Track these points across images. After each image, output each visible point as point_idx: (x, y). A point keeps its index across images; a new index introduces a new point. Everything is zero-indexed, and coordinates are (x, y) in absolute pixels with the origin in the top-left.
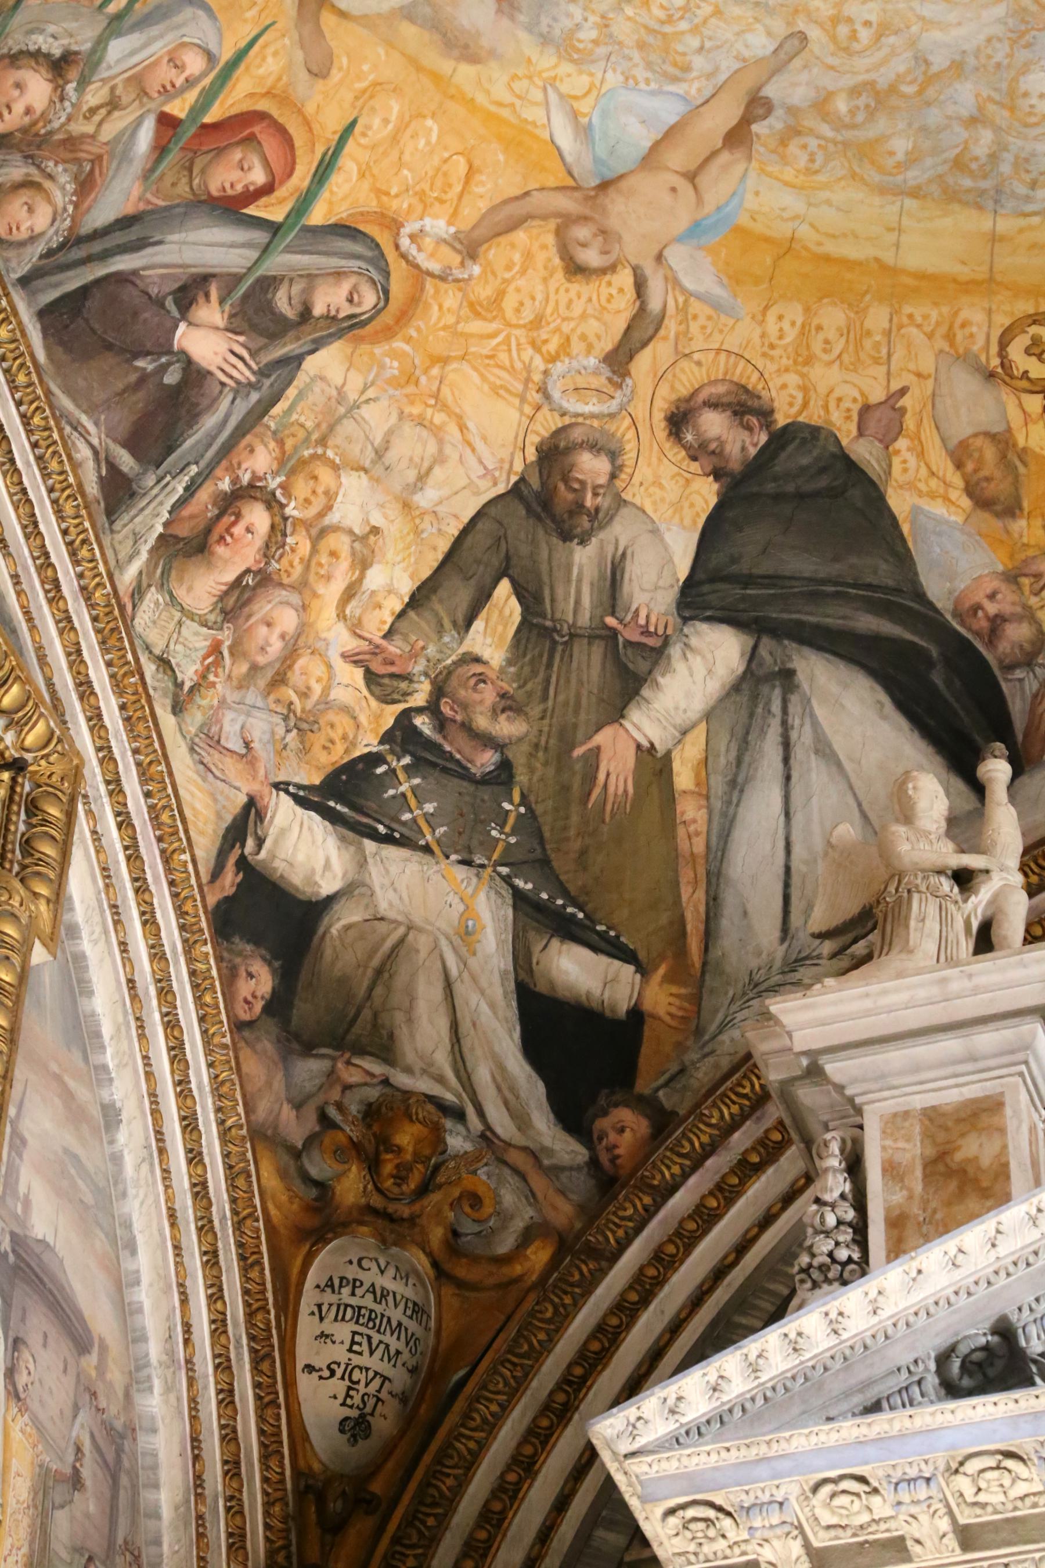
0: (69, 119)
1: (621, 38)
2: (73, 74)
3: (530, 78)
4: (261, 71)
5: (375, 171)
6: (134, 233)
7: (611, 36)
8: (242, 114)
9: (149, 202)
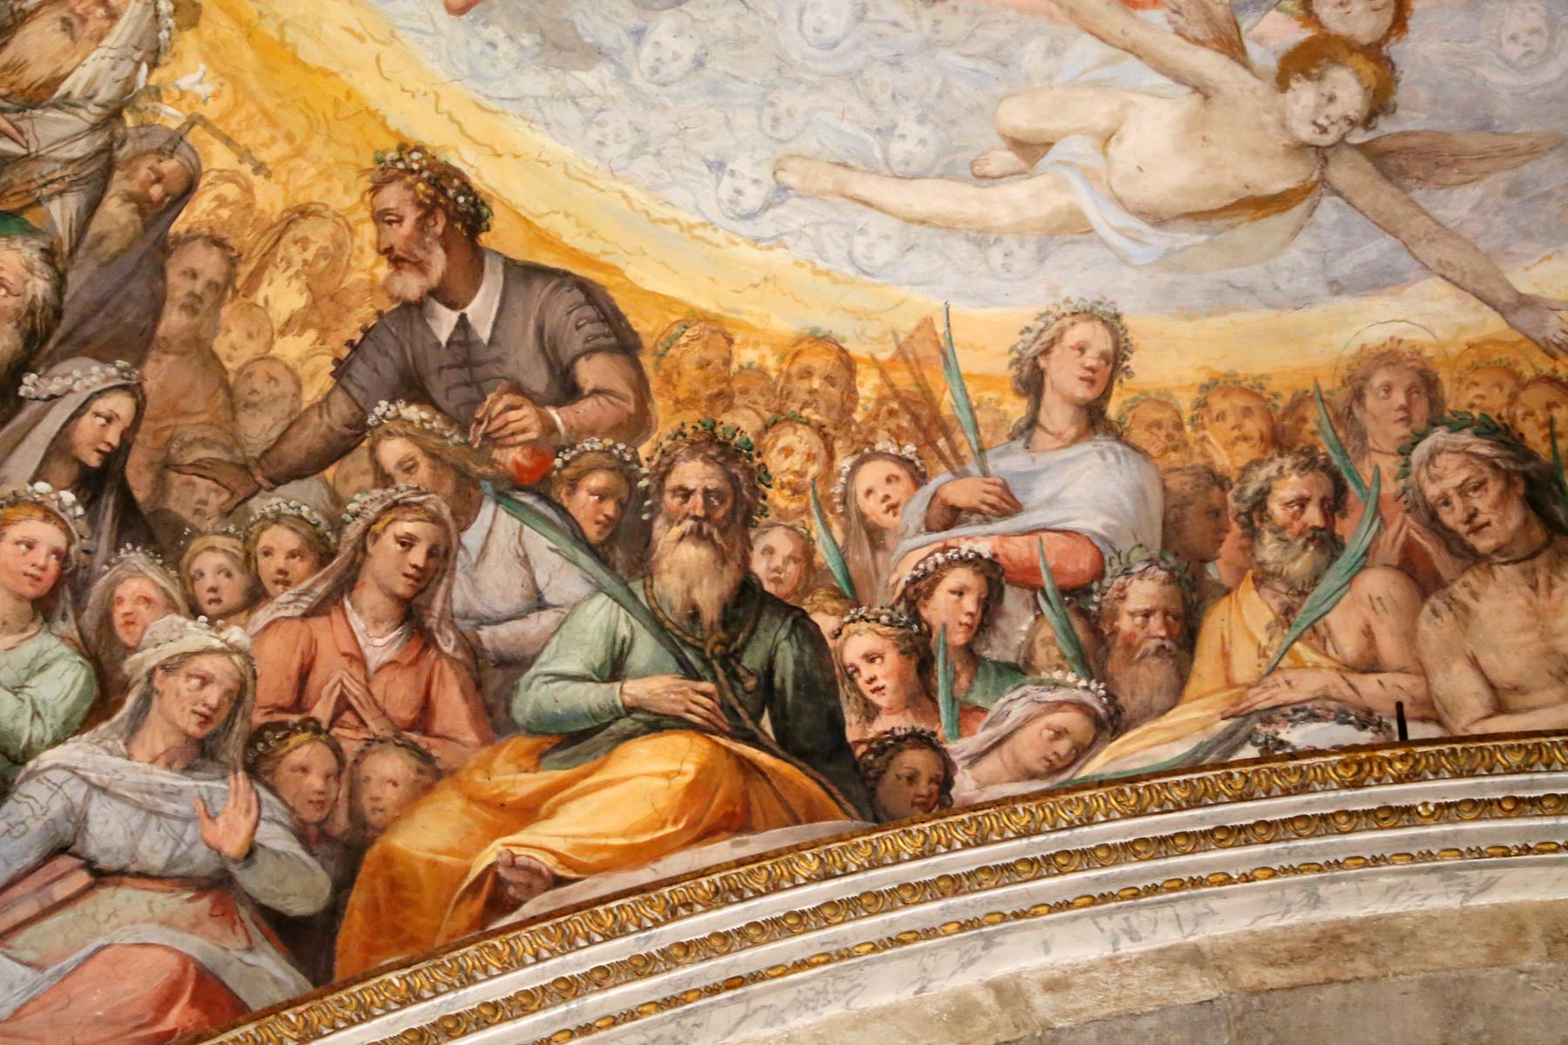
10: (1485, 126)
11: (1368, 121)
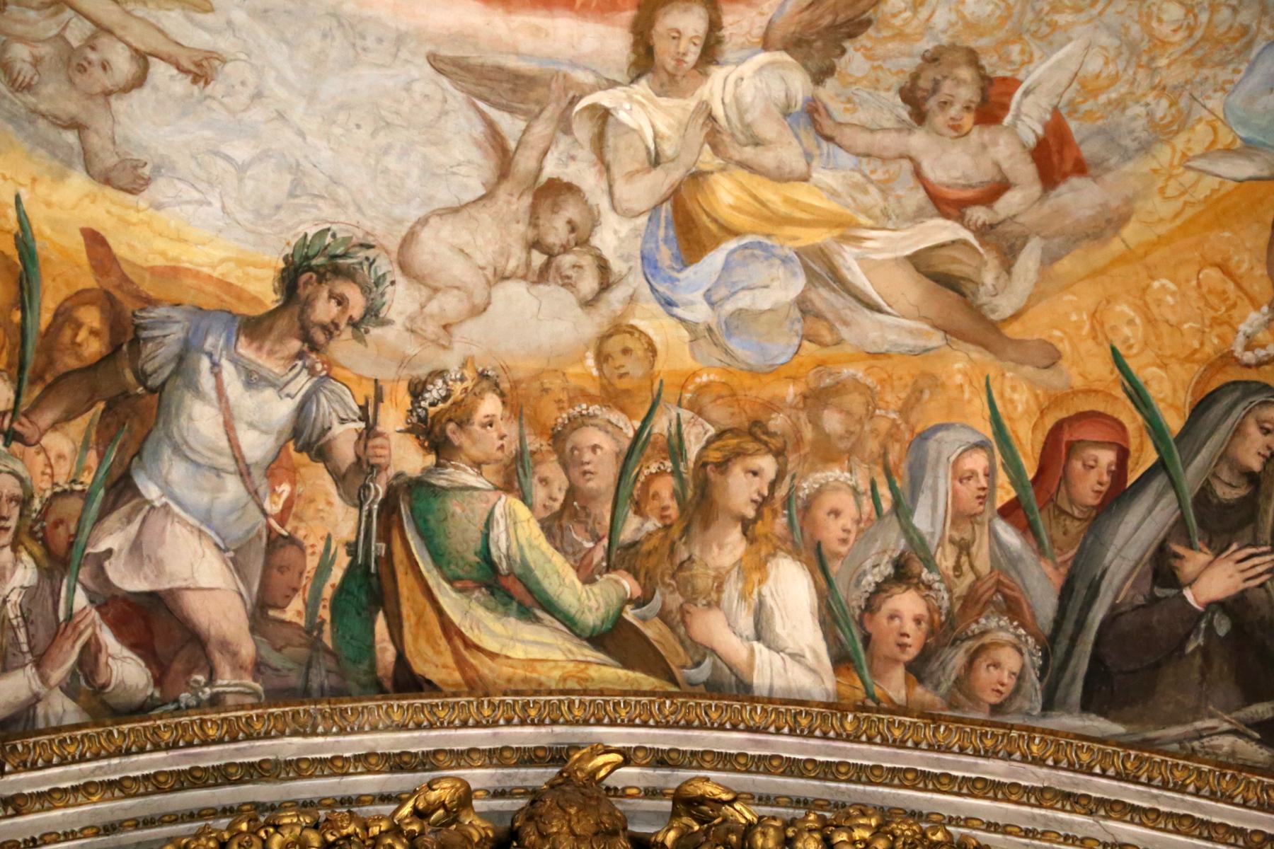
0: (949, 590)
1: (1181, 79)
2: (916, 566)
3: (1170, 177)
4: (1020, 408)
5: (1168, 352)
6: (1081, 590)
7: (1175, 88)
8: (1045, 443)
9: (1065, 562)
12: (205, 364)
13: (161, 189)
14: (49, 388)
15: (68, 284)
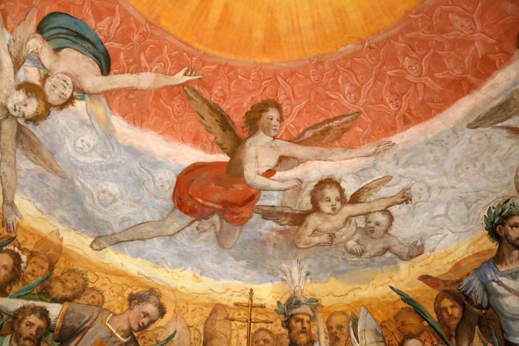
10: (53, 153)
11: (28, 120)
12: (495, 284)
13: (429, 245)
14: (456, 337)
15: (430, 299)
